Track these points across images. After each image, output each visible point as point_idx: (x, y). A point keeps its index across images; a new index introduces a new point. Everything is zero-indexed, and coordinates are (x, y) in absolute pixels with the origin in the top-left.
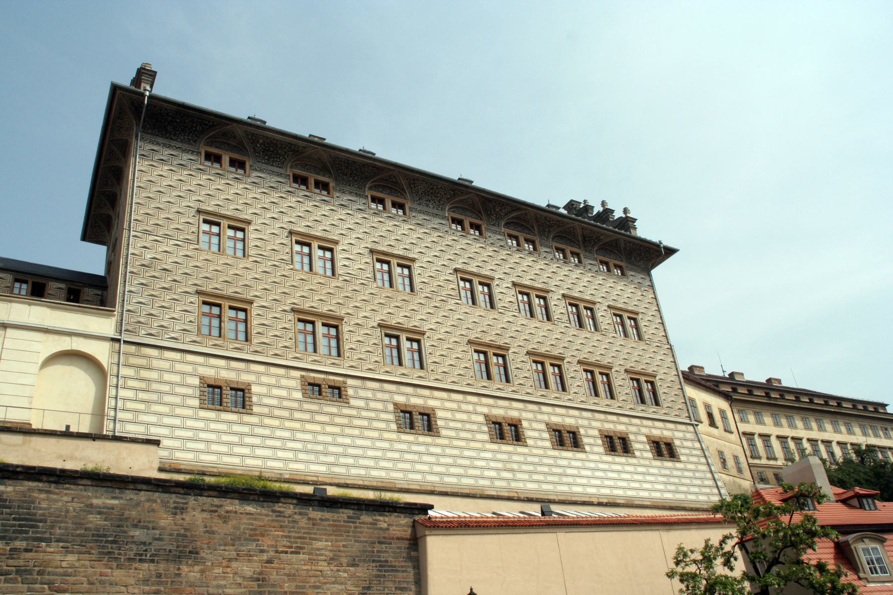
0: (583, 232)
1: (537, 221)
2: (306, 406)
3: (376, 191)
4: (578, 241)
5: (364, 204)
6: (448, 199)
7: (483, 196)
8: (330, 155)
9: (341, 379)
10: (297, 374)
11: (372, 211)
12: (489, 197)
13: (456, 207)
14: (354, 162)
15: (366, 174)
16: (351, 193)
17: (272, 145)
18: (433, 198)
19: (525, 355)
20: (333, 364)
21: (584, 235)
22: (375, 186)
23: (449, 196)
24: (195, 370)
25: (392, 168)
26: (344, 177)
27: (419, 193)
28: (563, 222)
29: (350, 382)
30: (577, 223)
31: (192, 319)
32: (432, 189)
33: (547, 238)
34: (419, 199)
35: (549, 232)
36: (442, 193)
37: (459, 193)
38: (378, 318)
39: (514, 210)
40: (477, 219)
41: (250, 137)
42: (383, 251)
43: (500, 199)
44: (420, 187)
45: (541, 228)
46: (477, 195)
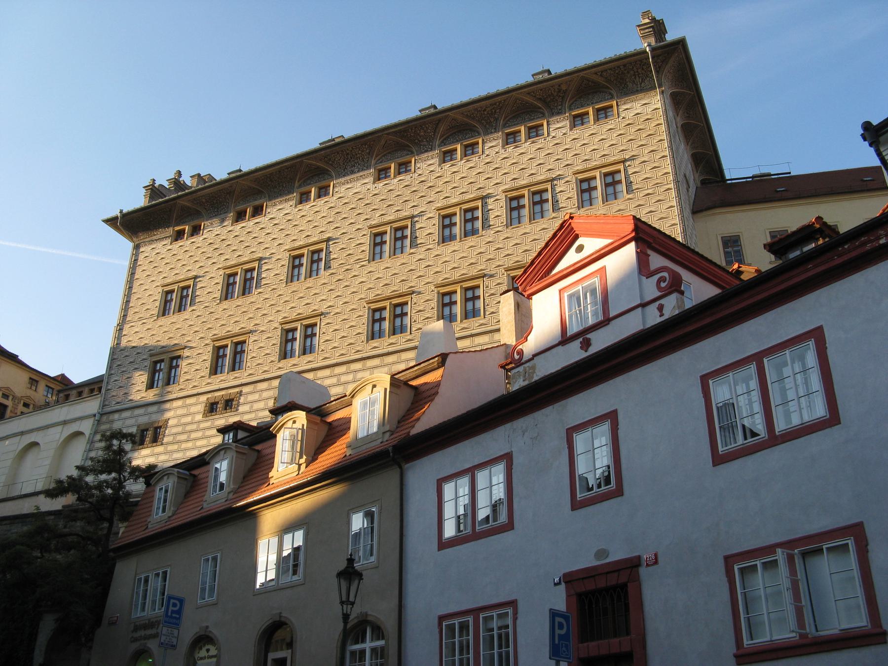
0: (535, 96)
1: (473, 118)
2: (203, 425)
3: (305, 186)
4: (540, 108)
5: (291, 206)
6: (369, 154)
7: (393, 132)
8: (250, 180)
9: (237, 390)
10: (203, 398)
11: (297, 210)
12: (399, 128)
13: (384, 156)
14: (271, 174)
15: (289, 176)
16: (281, 201)
17: (212, 198)
18: (356, 161)
19: (433, 291)
20: (236, 378)
21: (540, 99)
22: (304, 182)
23: (367, 151)
24: (136, 421)
25: (298, 160)
26: (276, 190)
27: (341, 164)
28: (500, 102)
29: (245, 389)
30: (514, 93)
31: (143, 380)
32: (348, 154)
33: (495, 129)
34: (344, 170)
35: (496, 119)
36: (360, 152)
37: (372, 143)
38: (280, 319)
39: (438, 124)
40: (408, 154)
41: (195, 202)
42: (300, 245)
43: (410, 124)
44: (337, 159)
45: (483, 121)
46: (388, 134)
